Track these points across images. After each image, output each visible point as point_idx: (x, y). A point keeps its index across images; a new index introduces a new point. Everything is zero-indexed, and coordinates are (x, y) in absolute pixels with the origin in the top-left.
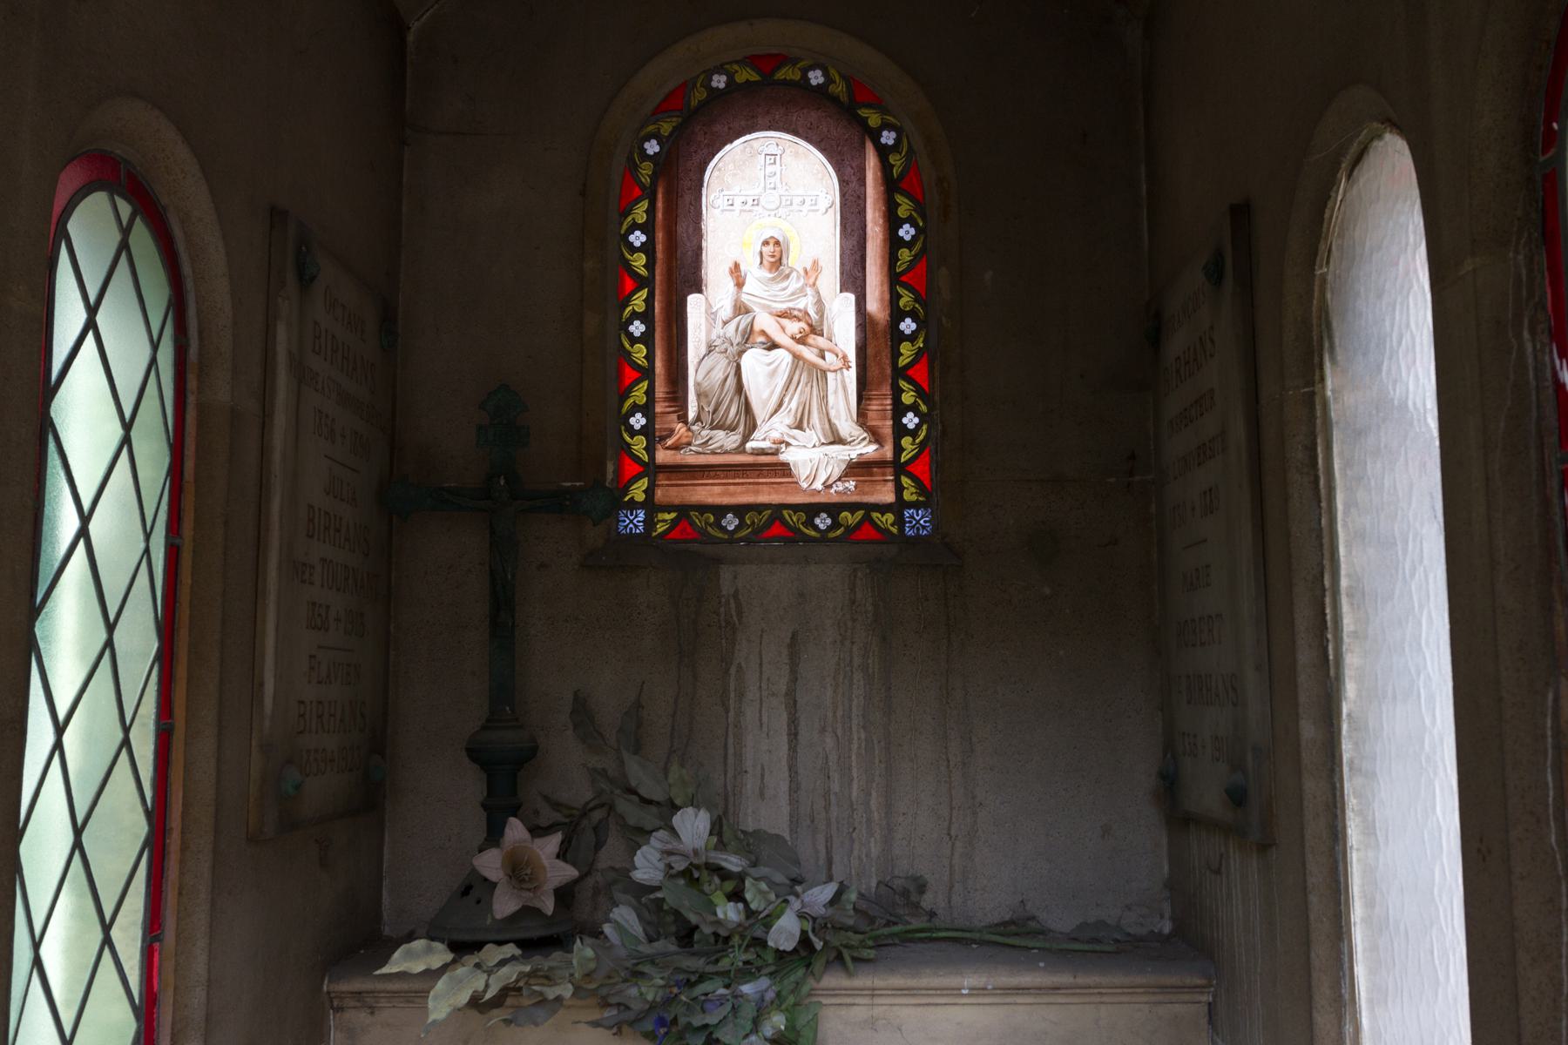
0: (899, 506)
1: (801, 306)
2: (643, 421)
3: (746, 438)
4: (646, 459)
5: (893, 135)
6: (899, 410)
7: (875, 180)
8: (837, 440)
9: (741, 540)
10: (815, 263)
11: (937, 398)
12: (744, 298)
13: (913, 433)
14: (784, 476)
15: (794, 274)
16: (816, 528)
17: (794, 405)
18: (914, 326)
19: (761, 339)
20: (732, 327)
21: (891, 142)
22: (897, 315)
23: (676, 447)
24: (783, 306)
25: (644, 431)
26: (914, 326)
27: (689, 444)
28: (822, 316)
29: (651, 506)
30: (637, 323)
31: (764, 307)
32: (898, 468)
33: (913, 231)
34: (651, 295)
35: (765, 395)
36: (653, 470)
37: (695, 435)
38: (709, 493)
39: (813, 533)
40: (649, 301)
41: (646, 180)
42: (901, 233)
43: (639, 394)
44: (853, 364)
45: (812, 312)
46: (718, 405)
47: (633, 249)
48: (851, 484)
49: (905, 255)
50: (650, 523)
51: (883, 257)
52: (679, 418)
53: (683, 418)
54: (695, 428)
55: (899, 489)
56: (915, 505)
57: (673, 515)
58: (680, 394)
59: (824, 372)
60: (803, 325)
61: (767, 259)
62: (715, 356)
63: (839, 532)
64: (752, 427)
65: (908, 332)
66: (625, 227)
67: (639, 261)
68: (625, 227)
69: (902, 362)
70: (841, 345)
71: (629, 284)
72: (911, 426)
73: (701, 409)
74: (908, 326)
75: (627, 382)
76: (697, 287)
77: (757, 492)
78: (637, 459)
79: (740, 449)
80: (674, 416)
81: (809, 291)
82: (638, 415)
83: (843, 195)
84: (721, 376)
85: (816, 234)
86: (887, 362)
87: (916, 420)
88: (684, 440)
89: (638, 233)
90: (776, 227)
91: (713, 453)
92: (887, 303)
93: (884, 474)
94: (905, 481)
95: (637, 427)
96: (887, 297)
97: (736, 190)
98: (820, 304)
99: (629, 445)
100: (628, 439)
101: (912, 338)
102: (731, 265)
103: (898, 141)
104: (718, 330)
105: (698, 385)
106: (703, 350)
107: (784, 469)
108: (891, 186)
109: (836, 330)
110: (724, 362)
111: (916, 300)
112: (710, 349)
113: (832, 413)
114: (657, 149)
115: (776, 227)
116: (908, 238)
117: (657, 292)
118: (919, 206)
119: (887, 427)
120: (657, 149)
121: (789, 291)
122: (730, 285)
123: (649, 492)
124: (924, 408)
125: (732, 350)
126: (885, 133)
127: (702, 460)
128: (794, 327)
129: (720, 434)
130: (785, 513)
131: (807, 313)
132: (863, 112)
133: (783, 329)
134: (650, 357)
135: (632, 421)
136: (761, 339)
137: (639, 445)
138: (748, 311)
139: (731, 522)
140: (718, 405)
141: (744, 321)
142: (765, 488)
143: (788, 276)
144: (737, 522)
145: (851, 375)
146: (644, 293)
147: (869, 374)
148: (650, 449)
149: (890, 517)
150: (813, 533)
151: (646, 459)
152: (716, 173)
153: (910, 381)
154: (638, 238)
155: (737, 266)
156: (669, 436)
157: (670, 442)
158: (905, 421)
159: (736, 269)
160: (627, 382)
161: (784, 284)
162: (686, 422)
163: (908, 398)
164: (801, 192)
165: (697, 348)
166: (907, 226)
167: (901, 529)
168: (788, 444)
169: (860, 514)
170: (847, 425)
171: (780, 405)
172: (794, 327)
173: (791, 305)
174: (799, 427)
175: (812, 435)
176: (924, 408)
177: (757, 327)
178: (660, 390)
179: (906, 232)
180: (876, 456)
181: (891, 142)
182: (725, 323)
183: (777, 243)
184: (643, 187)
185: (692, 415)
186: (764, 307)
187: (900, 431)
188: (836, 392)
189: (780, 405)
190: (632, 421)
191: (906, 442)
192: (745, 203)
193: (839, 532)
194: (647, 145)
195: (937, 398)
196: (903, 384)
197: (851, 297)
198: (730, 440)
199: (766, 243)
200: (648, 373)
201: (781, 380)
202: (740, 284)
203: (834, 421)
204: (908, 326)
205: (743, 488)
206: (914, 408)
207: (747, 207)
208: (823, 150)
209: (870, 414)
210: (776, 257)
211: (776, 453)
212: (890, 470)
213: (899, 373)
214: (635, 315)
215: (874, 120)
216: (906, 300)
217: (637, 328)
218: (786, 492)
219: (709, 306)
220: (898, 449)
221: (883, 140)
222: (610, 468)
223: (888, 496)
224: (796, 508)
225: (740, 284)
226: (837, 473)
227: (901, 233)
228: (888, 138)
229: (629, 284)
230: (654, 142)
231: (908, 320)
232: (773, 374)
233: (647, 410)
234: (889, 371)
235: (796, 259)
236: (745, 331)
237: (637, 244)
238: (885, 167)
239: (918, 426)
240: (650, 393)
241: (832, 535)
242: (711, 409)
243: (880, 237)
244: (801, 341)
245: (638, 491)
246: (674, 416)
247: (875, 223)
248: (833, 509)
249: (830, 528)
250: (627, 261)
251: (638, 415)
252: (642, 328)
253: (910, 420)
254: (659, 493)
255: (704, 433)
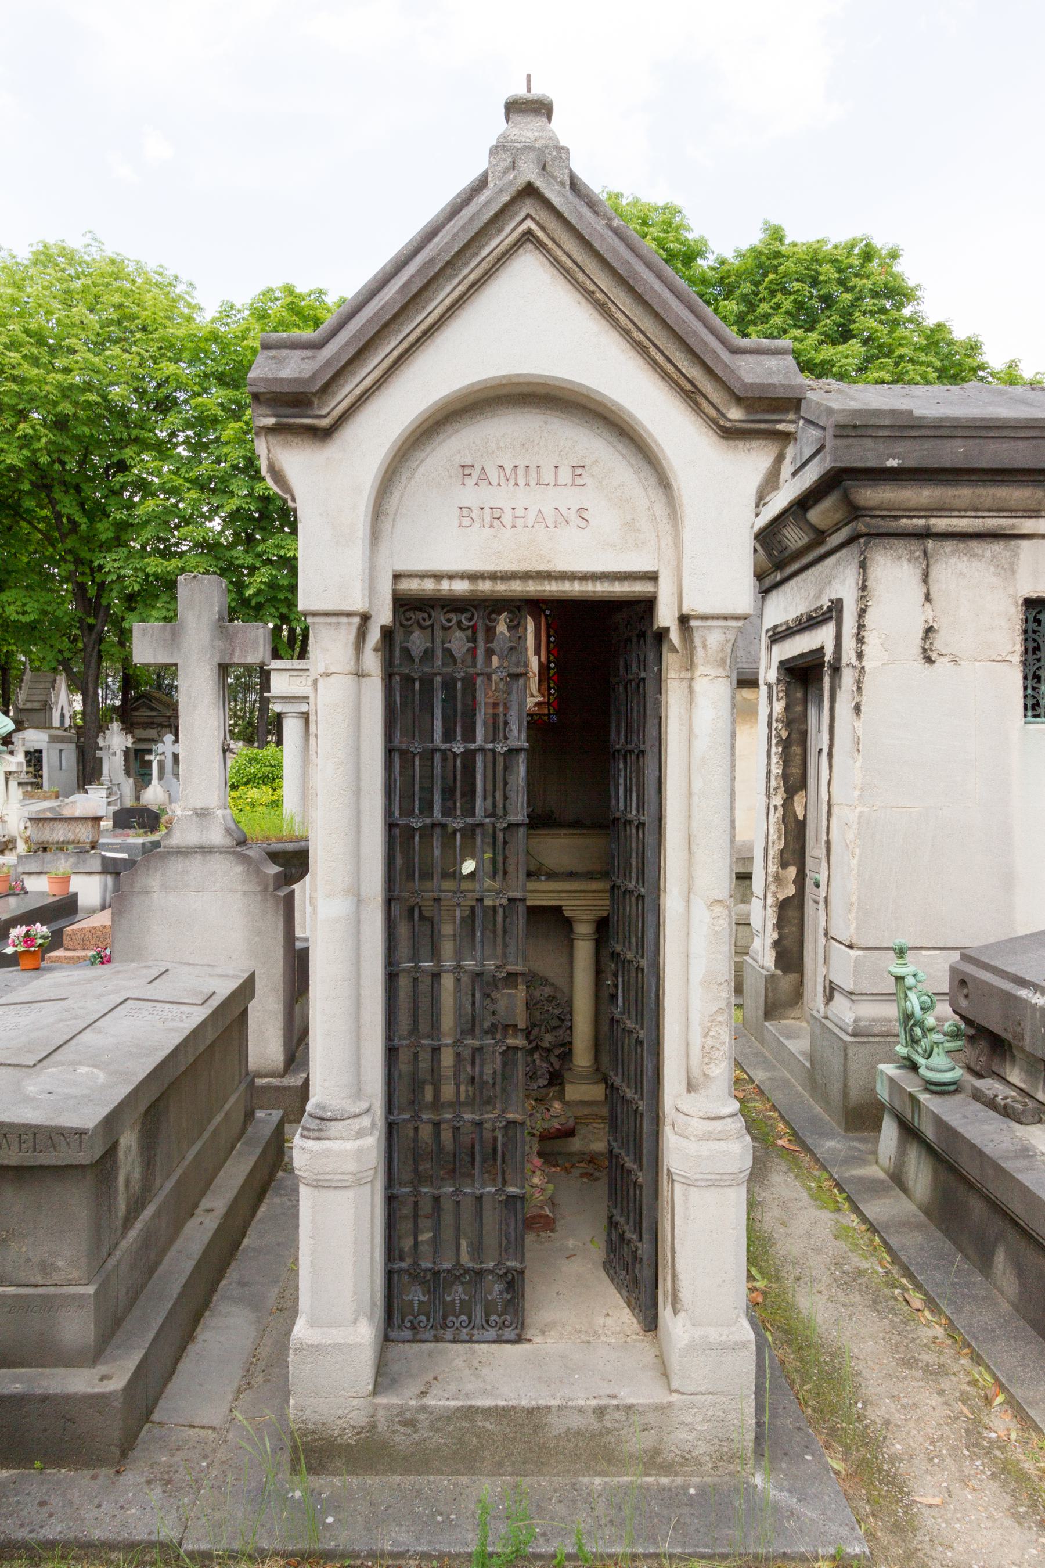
0: (549, 714)
6: (549, 688)
22: (549, 662)
108: (548, 626)
118: (556, 632)
145: (537, 679)
163: (552, 685)
170: (535, 693)
187: (549, 694)
216: (552, 658)
223: (546, 712)
228: (548, 612)
238: (546, 619)
253: (552, 691)
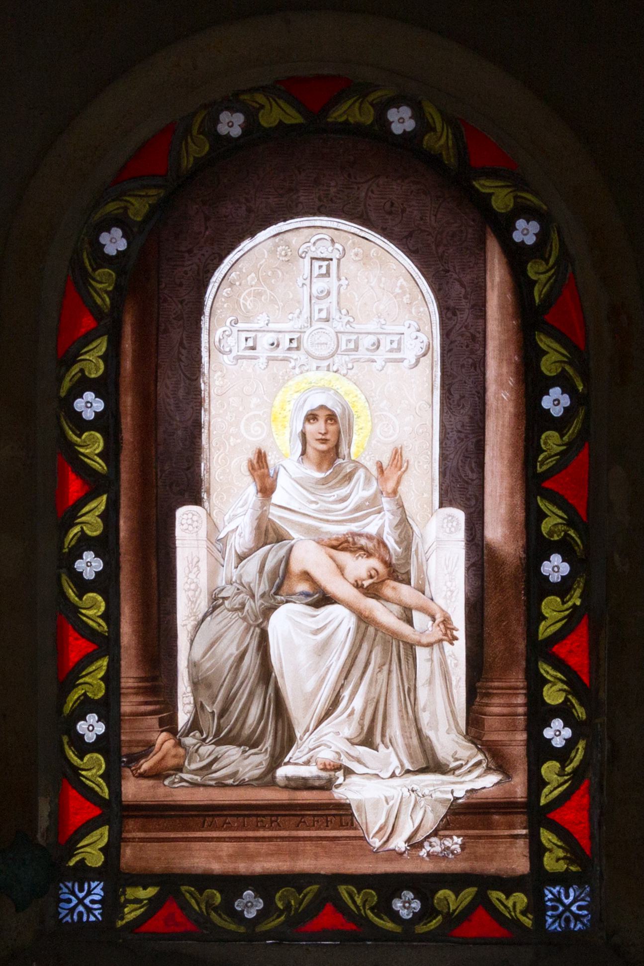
0: (536, 880)
1: (372, 530)
2: (101, 728)
3: (277, 760)
4: (106, 794)
5: (534, 227)
6: (539, 714)
7: (501, 307)
8: (432, 764)
9: (267, 935)
10: (452, 644)
11: (603, 695)
12: (275, 514)
13: (562, 755)
14: (341, 826)
15: (361, 473)
16: (395, 916)
17: (358, 703)
18: (565, 569)
19: (303, 587)
20: (252, 565)
21: (530, 240)
22: (537, 547)
23: (157, 774)
24: (341, 530)
25: (103, 744)
26: (565, 569)
27: (179, 769)
28: (408, 549)
29: (114, 875)
30: (88, 556)
31: (309, 530)
32: (535, 813)
33: (566, 401)
34: (113, 508)
35: (310, 685)
36: (117, 813)
37: (189, 754)
38: (210, 855)
39: (389, 925)
40: (110, 517)
41: (104, 301)
42: (546, 402)
43: (93, 682)
44: (461, 634)
45: (391, 542)
46: (229, 702)
47: (81, 425)
48: (455, 842)
49: (552, 442)
50: (112, 904)
51: (514, 445)
52: (162, 723)
53: (169, 723)
54: (189, 741)
55: (537, 851)
56: (564, 879)
57: (151, 891)
58: (163, 682)
59: (411, 647)
60: (374, 563)
61: (315, 446)
62: (223, 617)
63: (434, 923)
64: (286, 740)
65: (555, 578)
66: (66, 384)
67: (92, 446)
68: (66, 384)
69: (545, 630)
70: (440, 601)
71: (75, 487)
72: (558, 743)
73: (199, 707)
74: (555, 567)
75: (74, 657)
76: (192, 491)
77: (295, 854)
78: (90, 794)
79: (267, 779)
80: (153, 721)
81: (386, 503)
82: (92, 718)
83: (446, 334)
84: (233, 651)
85: (396, 395)
86: (518, 629)
87: (567, 733)
88: (171, 762)
89: (89, 396)
90: (325, 370)
91: (221, 784)
92: (520, 527)
93: (512, 826)
94: (547, 837)
95: (90, 738)
96: (520, 515)
97: (260, 323)
98: (404, 527)
99: (76, 770)
100: (75, 760)
101: (563, 589)
102: (252, 455)
103: (543, 237)
104: (228, 571)
105: (193, 665)
106: (203, 605)
107: (342, 814)
108: (529, 318)
109: (432, 571)
110: (238, 627)
111: (570, 523)
112: (216, 603)
113: (425, 718)
114: (122, 245)
115: (325, 370)
116: (557, 412)
117: (124, 501)
118: (578, 356)
119: (517, 743)
120: (122, 245)
121: (352, 503)
122: (251, 491)
123: (111, 851)
124: (580, 712)
125: (254, 606)
126: (521, 224)
127: (201, 797)
128: (360, 567)
129: (232, 752)
130: (343, 890)
131: (382, 543)
132: (483, 185)
133: (341, 569)
134: (111, 616)
135: (81, 727)
136: (303, 587)
137: (93, 768)
138: (280, 537)
139: (250, 904)
140: (229, 702)
141: (274, 554)
142: (309, 846)
143: (349, 477)
144: (260, 904)
145: (457, 653)
146: (100, 503)
147: (488, 650)
148: (113, 777)
149: (520, 899)
150: (389, 925)
151: (106, 794)
152: (225, 291)
153: (558, 664)
154: (90, 405)
155: (261, 457)
156: (145, 754)
157: (146, 765)
158: (548, 733)
159: (260, 465)
160: (74, 657)
161: (343, 491)
162: (173, 731)
163: (553, 695)
164: (372, 326)
165: (193, 602)
166: (556, 392)
167: (540, 920)
168: (348, 772)
169: (469, 893)
170: (449, 742)
171: (335, 703)
172: (360, 567)
173: (354, 527)
174: (368, 741)
175: (390, 757)
176: (580, 712)
177: (296, 567)
178: (129, 675)
179: (555, 401)
180: (498, 794)
181: (530, 240)
182: (241, 558)
183: (332, 417)
184: (96, 311)
185: (183, 718)
186: (309, 530)
187: (540, 752)
188: (430, 682)
189: (335, 703)
190: (81, 727)
191: (549, 770)
192: (275, 345)
193: (434, 923)
194: (104, 238)
195: (603, 695)
196: (546, 670)
197: (459, 516)
198: (243, 763)
199: (312, 417)
200: (108, 644)
201: (336, 661)
202: (266, 490)
203: (428, 732)
204: (555, 567)
205: (272, 846)
206: (564, 712)
207: (279, 353)
208: (411, 253)
209: (489, 721)
210: (328, 440)
211: (328, 786)
212: (521, 819)
213: (539, 650)
214: (85, 543)
215: (502, 199)
216: (553, 522)
217: (90, 565)
218: (345, 855)
219: (213, 527)
220: (536, 783)
221: (517, 237)
222: (44, 809)
223: (521, 865)
224: (361, 881)
225: (266, 490)
226: (430, 824)
227: (546, 402)
228: (526, 232)
229: (75, 487)
230: (117, 232)
231: (556, 559)
232: (323, 649)
233: (107, 708)
234: (521, 646)
235: (363, 446)
236: (275, 572)
237: (89, 415)
238: (521, 285)
239: (570, 743)
240: (112, 678)
241: (421, 929)
242: (216, 708)
243: (509, 409)
244: (373, 591)
245: (92, 849)
246: (153, 721)
247: (501, 385)
248: (424, 885)
249: (419, 917)
250: (71, 445)
251: (92, 718)
252: (98, 565)
253: (557, 733)
254: (128, 852)
255: (205, 750)
